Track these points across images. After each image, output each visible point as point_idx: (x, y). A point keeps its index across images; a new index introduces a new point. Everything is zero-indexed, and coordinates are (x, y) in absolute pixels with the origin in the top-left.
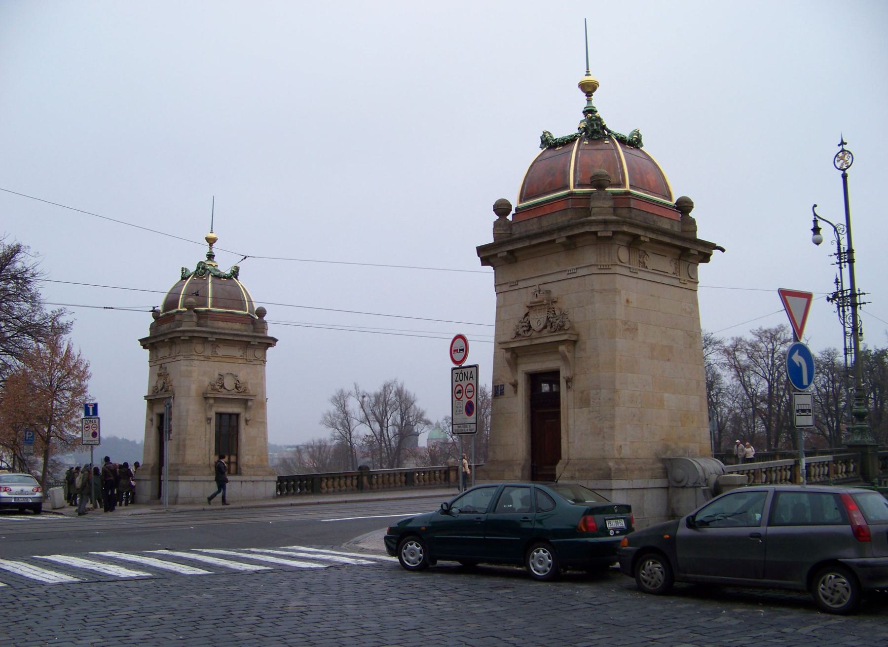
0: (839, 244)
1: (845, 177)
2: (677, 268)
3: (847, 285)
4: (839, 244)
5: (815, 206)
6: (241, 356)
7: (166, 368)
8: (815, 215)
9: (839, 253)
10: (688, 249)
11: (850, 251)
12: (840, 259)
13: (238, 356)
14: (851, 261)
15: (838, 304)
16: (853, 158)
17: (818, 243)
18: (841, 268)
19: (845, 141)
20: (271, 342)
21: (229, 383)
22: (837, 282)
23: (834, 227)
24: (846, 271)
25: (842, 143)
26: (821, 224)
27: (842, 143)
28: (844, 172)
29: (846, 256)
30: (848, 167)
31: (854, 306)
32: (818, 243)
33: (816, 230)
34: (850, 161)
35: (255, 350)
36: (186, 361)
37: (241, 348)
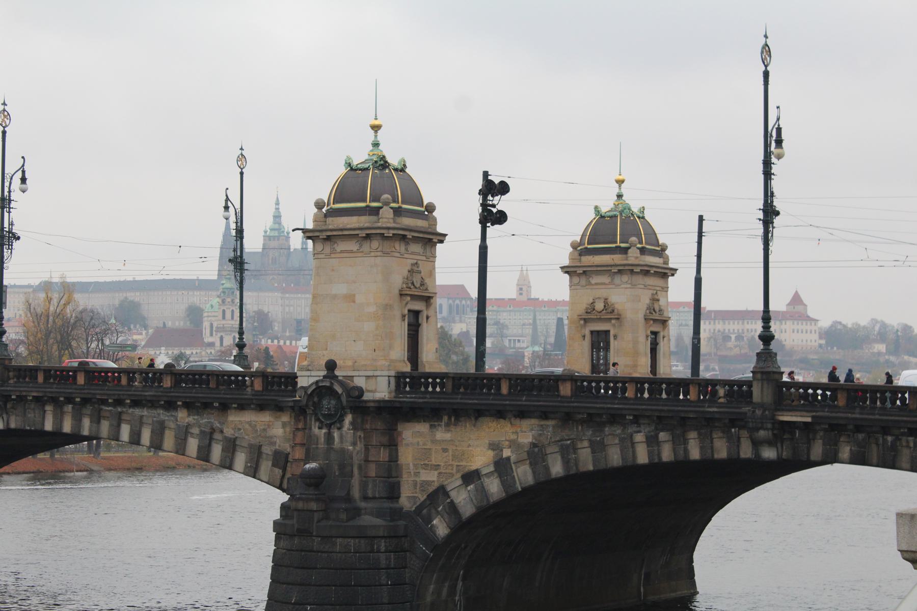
1: (242, 174)
2: (425, 249)
3: (239, 254)
5: (227, 189)
8: (227, 196)
10: (432, 239)
15: (234, 266)
16: (246, 162)
18: (236, 240)
19: (243, 148)
23: (236, 210)
24: (239, 242)
25: (242, 149)
27: (242, 149)
28: (242, 170)
30: (244, 168)
34: (245, 163)
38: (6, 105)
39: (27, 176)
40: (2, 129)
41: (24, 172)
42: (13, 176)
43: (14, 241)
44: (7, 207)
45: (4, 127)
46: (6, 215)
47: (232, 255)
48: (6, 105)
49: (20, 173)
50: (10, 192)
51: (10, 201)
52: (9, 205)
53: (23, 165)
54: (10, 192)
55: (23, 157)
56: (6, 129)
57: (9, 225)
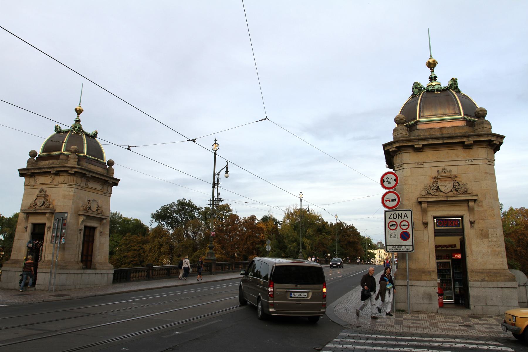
6: (101, 189)
7: (46, 191)
13: (99, 189)
20: (116, 182)
21: (94, 207)
35: (108, 187)
36: (68, 188)
37: (101, 184)
38: (217, 141)
39: (228, 170)
40: (214, 152)
41: (227, 168)
42: (219, 173)
43: (220, 202)
44: (216, 187)
45: (215, 151)
46: (216, 190)
48: (217, 141)
49: (225, 169)
50: (218, 180)
51: (218, 183)
52: (218, 185)
53: (227, 165)
54: (218, 180)
55: (227, 162)
56: (216, 152)
57: (217, 194)
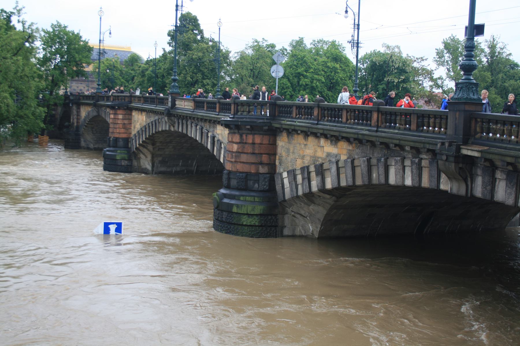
0: (355, 20)
3: (356, 38)
4: (355, 20)
9: (354, 24)
11: (358, 25)
12: (354, 26)
14: (358, 29)
17: (346, 17)
18: (354, 30)
22: (352, 36)
26: (348, 9)
29: (357, 26)
31: (358, 47)
32: (346, 17)
33: (346, 12)
47: (350, 39)
